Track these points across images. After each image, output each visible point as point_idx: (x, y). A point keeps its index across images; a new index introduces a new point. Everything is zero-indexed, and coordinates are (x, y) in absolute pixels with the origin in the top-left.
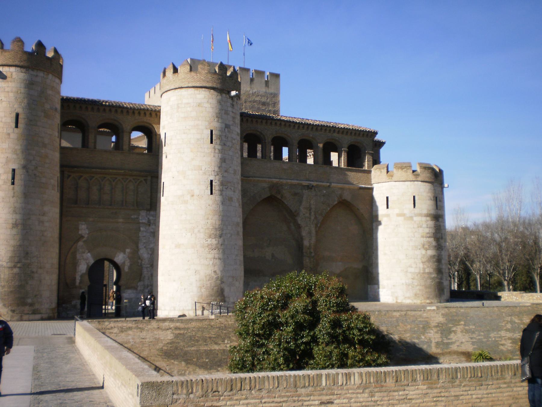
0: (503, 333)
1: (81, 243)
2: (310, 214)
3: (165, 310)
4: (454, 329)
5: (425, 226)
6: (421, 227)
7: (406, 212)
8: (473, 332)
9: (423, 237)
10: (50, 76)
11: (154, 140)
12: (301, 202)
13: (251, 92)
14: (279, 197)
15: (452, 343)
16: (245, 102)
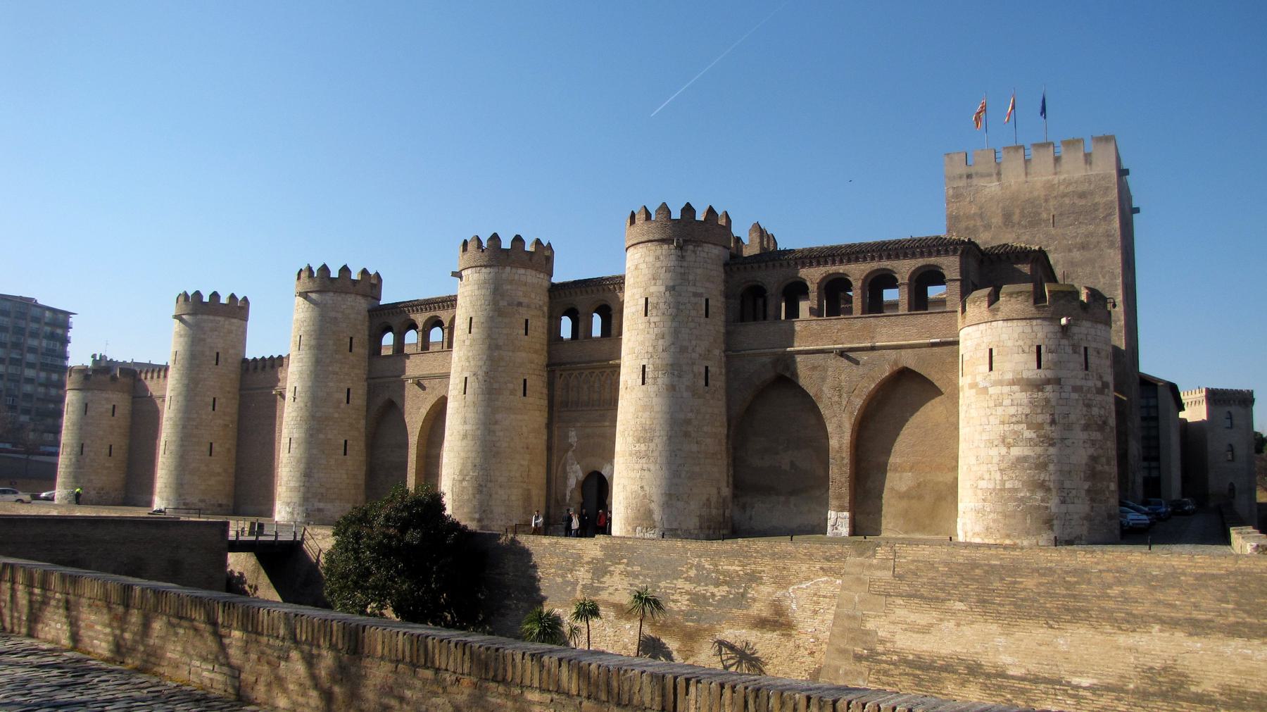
0: (680, 583)
1: (570, 453)
2: (840, 396)
3: (614, 533)
4: (612, 568)
5: (1007, 402)
6: (1001, 405)
7: (979, 379)
8: (636, 577)
9: (1003, 423)
10: (508, 269)
11: (614, 322)
12: (824, 379)
13: (1056, 181)
14: (788, 375)
15: (603, 589)
16: (1046, 201)
